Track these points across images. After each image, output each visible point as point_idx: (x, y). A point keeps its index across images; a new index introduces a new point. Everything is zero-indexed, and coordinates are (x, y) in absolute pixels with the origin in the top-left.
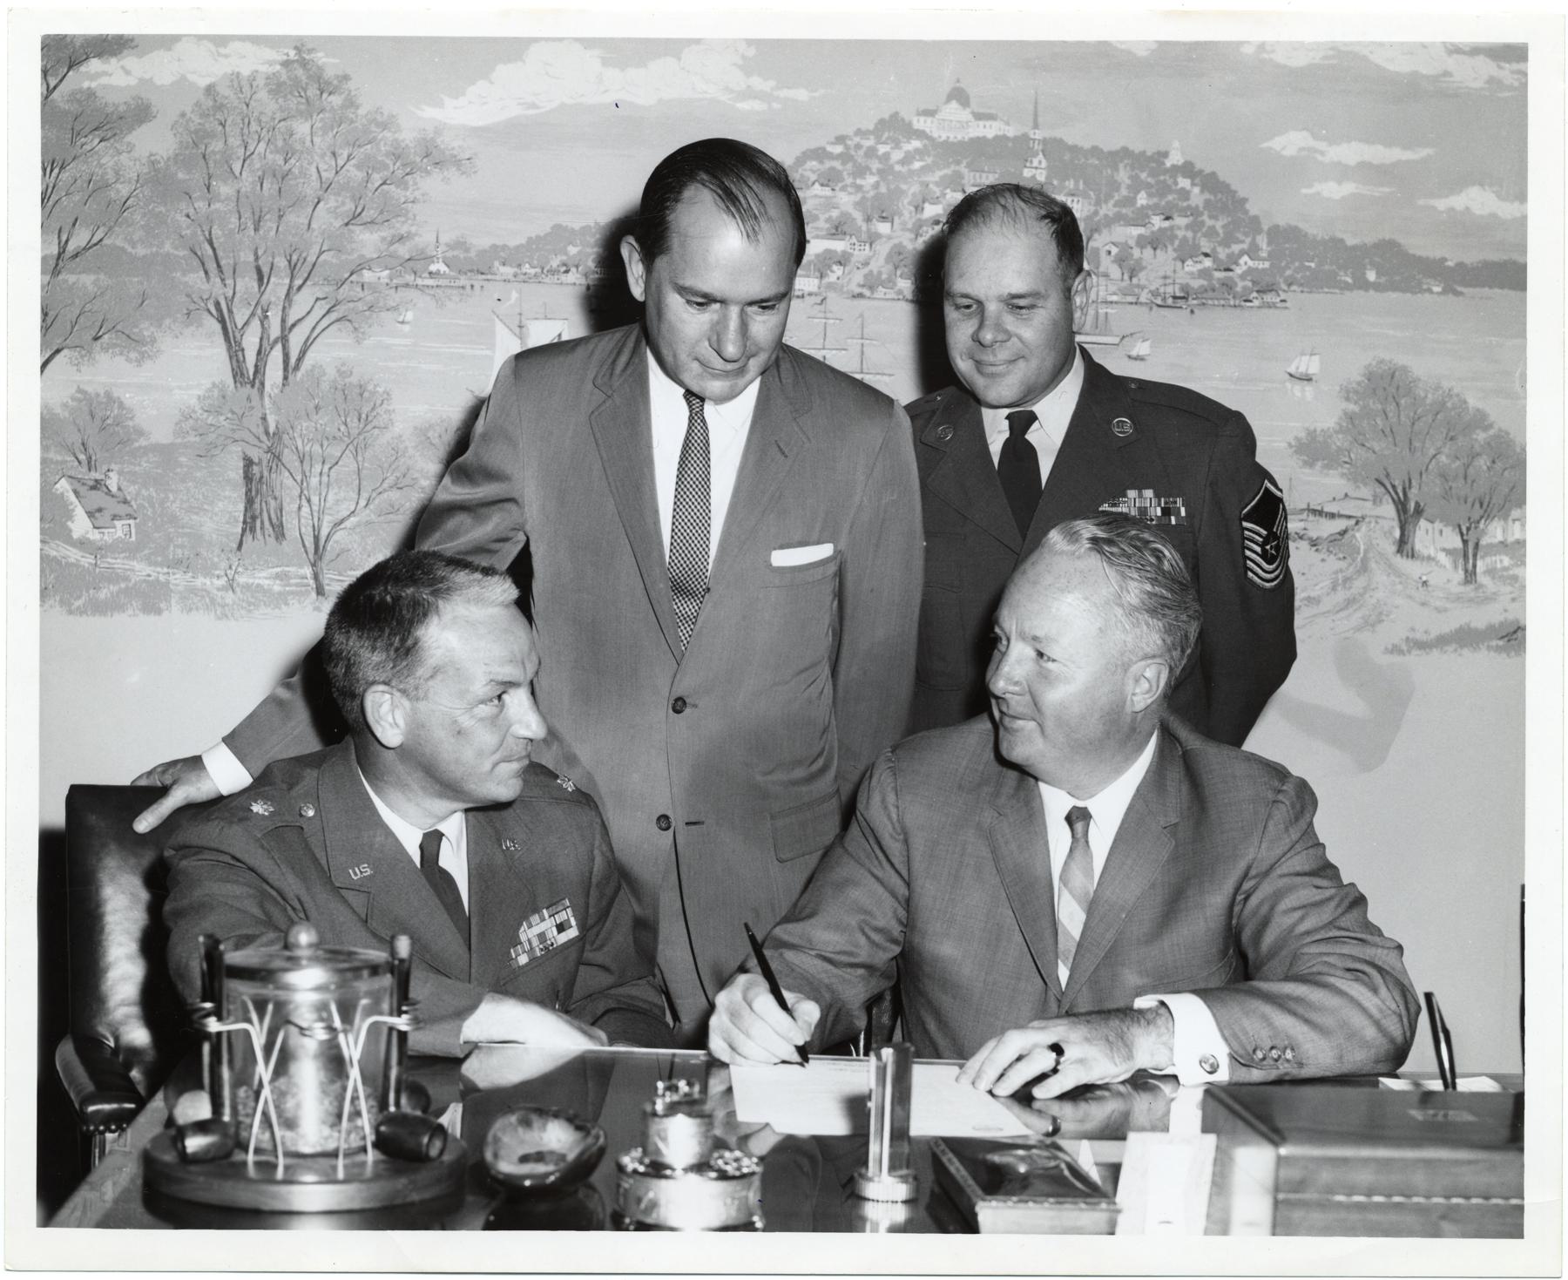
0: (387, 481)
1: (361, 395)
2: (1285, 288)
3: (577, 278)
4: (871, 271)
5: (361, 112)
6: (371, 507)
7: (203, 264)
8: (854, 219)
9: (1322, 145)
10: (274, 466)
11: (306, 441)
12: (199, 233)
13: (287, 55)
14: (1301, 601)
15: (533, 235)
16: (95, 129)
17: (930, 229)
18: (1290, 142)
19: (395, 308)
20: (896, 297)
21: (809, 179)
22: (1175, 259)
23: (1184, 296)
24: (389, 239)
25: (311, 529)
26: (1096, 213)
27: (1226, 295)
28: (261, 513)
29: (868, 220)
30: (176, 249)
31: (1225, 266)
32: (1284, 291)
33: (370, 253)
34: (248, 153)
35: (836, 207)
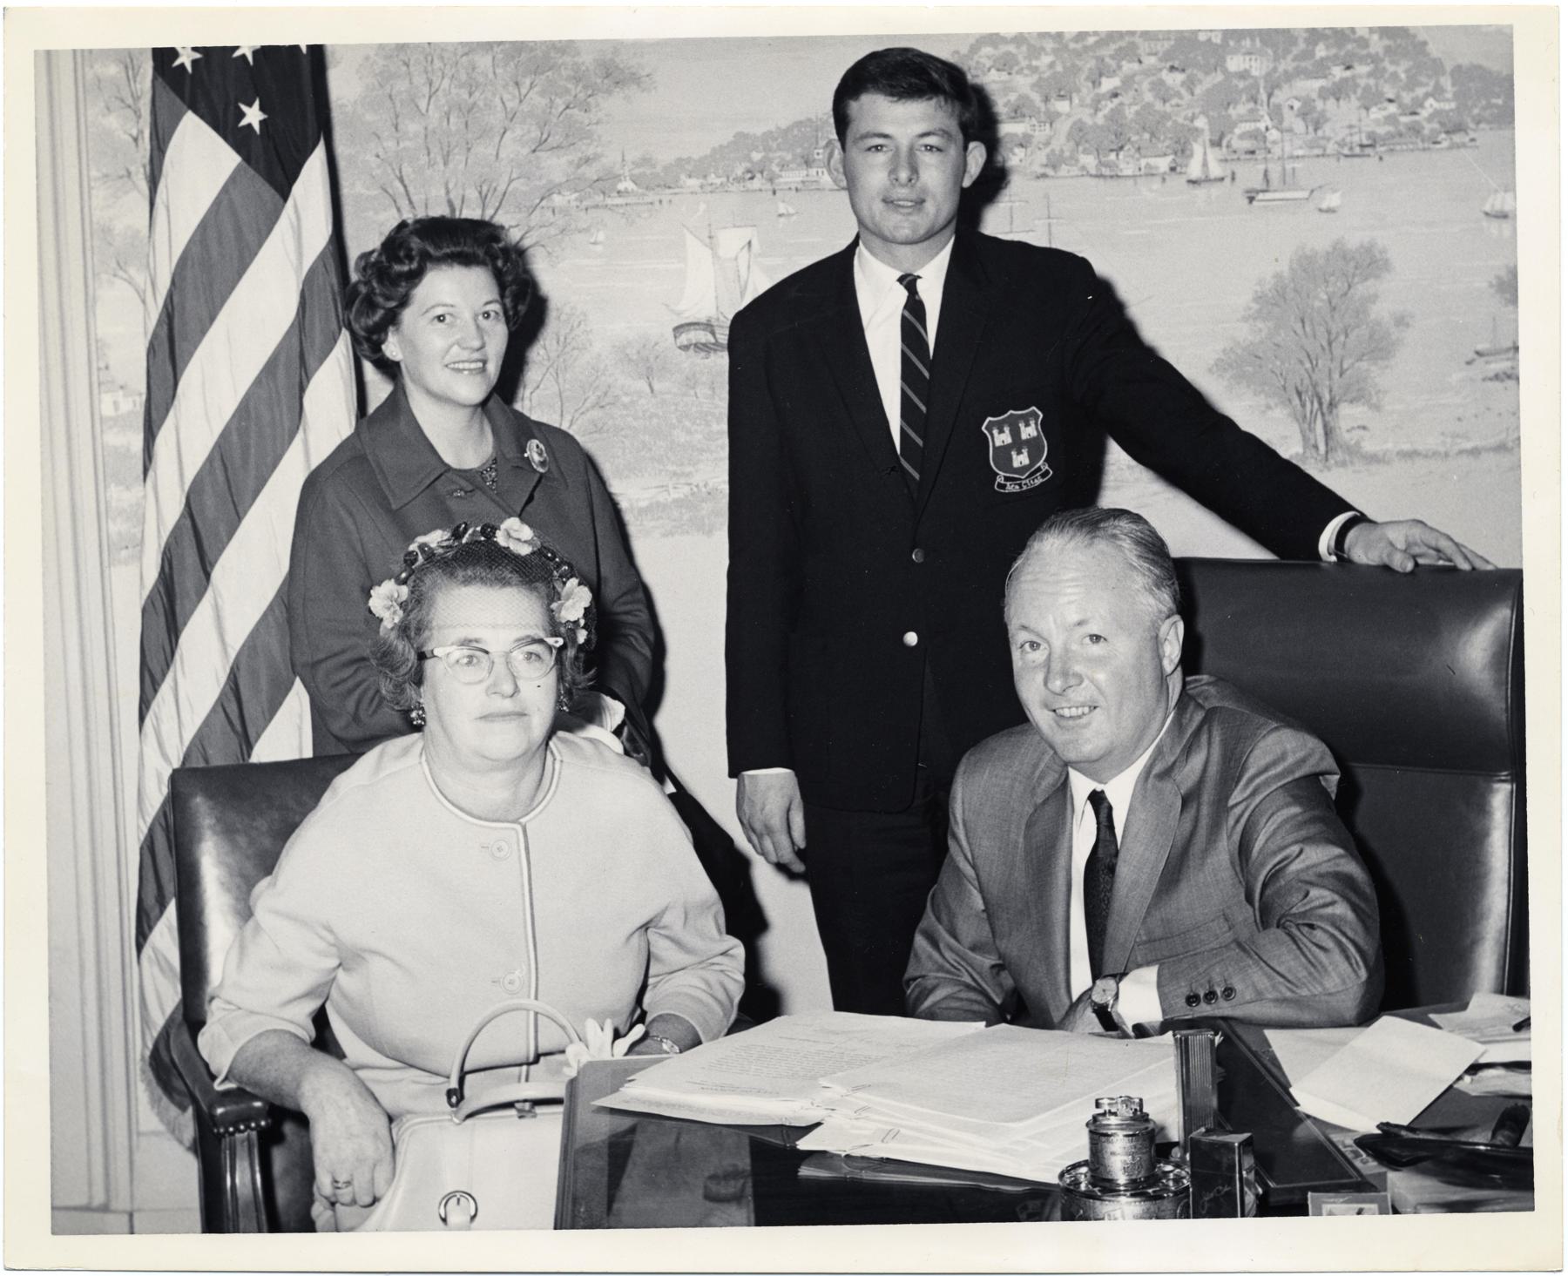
0: (589, 401)
2: (1472, 125)
3: (762, 184)
4: (1053, 151)
7: (395, 201)
8: (1032, 101)
12: (390, 171)
14: (1513, 441)
15: (717, 145)
17: (1109, 102)
19: (587, 230)
20: (1080, 173)
21: (984, 65)
22: (1359, 108)
23: (1373, 143)
24: (576, 162)
26: (1275, 69)
27: (1414, 139)
29: (1046, 100)
30: (368, 189)
31: (1411, 110)
32: (1474, 130)
33: (558, 177)
34: (433, 90)
35: (1013, 90)
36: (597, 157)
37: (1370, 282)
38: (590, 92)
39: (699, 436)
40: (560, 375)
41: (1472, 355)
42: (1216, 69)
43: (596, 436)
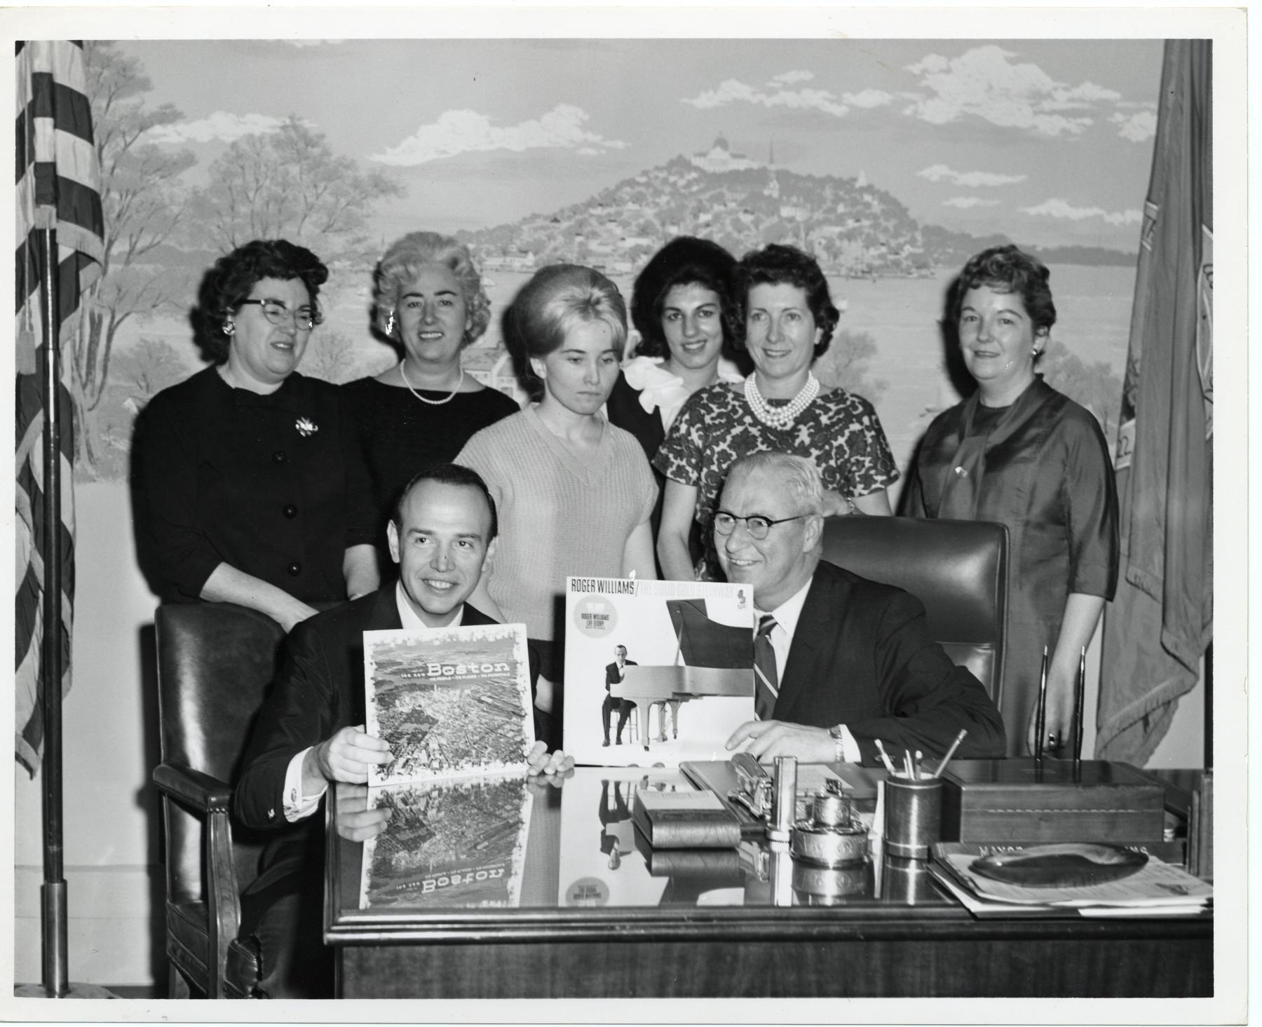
1: (333, 342)
2: (933, 264)
5: (333, 158)
9: (955, 174)
12: (226, 237)
13: (284, 122)
16: (158, 170)
18: (936, 172)
19: (355, 286)
23: (870, 270)
26: (811, 218)
29: (663, 224)
35: (643, 217)
36: (365, 239)
37: (863, 359)
38: (363, 195)
41: (923, 411)
42: (773, 214)
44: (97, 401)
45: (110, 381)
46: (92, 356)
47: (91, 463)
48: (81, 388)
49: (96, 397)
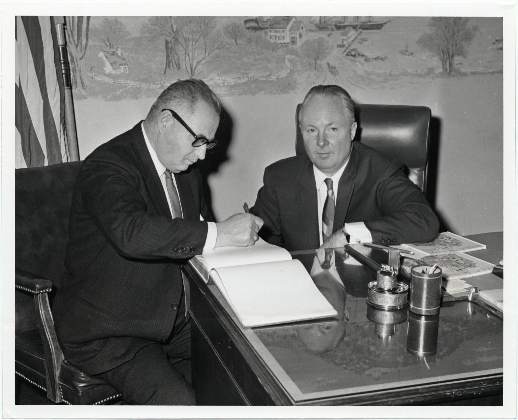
6: (210, 56)
10: (176, 43)
11: (187, 33)
25: (189, 65)
28: (172, 60)
39: (251, 60)
40: (205, 37)
41: (494, 41)
43: (217, 59)
44: (84, 54)
45: (90, 43)
46: (79, 29)
47: (84, 89)
48: (75, 47)
49: (84, 52)
